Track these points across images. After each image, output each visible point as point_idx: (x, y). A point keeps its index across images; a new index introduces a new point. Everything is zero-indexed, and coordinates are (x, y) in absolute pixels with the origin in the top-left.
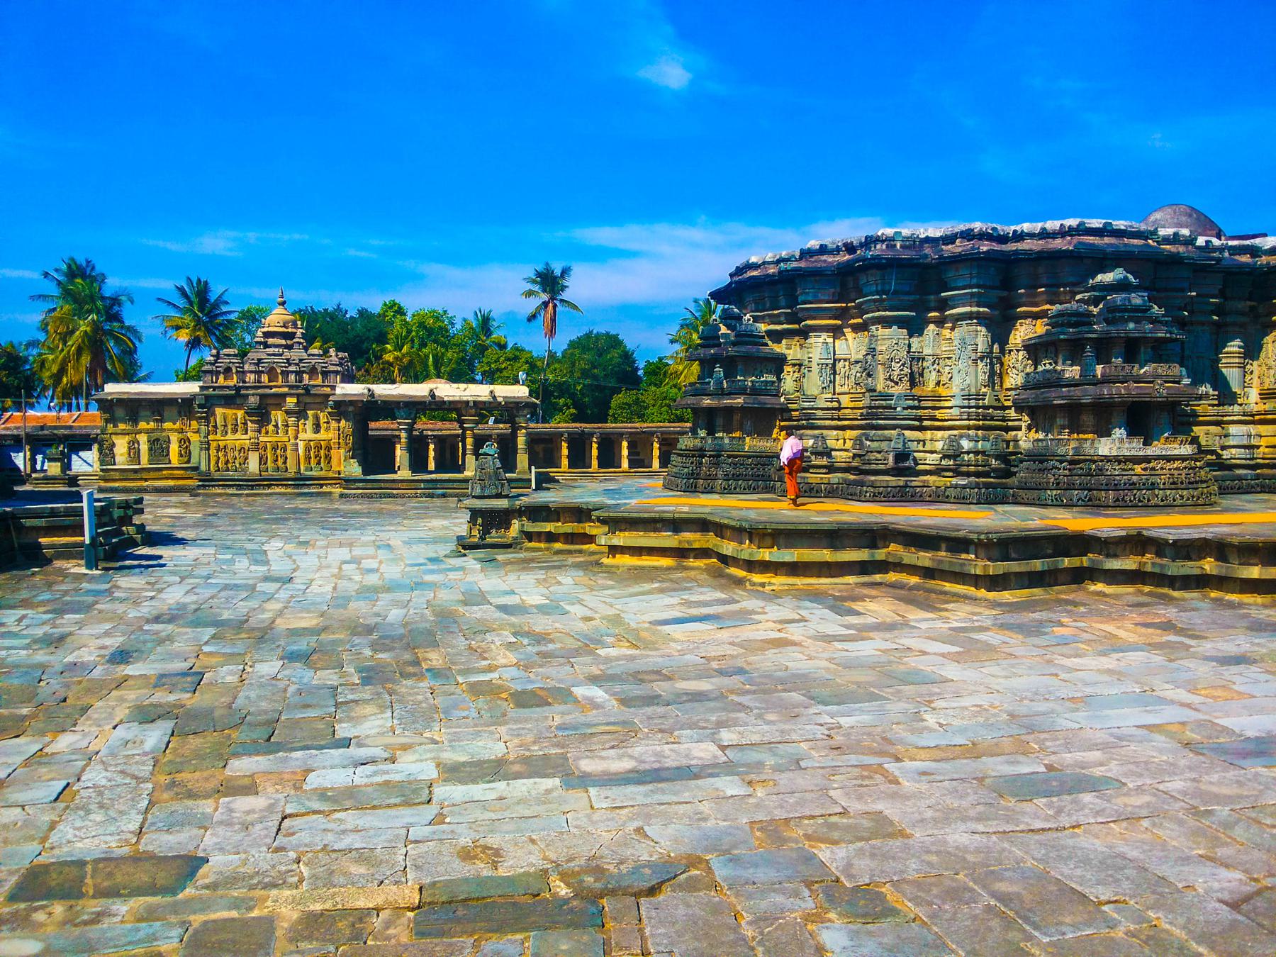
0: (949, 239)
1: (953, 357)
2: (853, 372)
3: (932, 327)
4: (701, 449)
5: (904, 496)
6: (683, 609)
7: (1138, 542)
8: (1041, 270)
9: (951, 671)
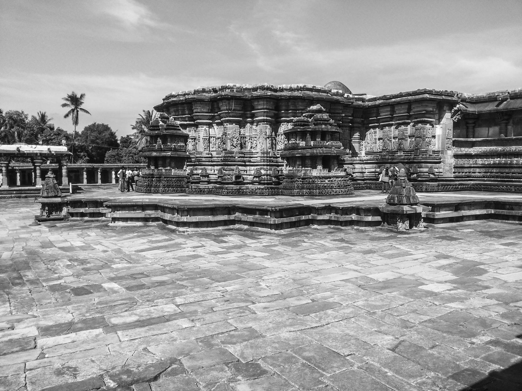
0: (255, 89)
1: (257, 138)
2: (217, 142)
3: (248, 124)
4: (152, 175)
5: (240, 193)
6: (150, 244)
7: (329, 209)
8: (290, 104)
9: (267, 263)
